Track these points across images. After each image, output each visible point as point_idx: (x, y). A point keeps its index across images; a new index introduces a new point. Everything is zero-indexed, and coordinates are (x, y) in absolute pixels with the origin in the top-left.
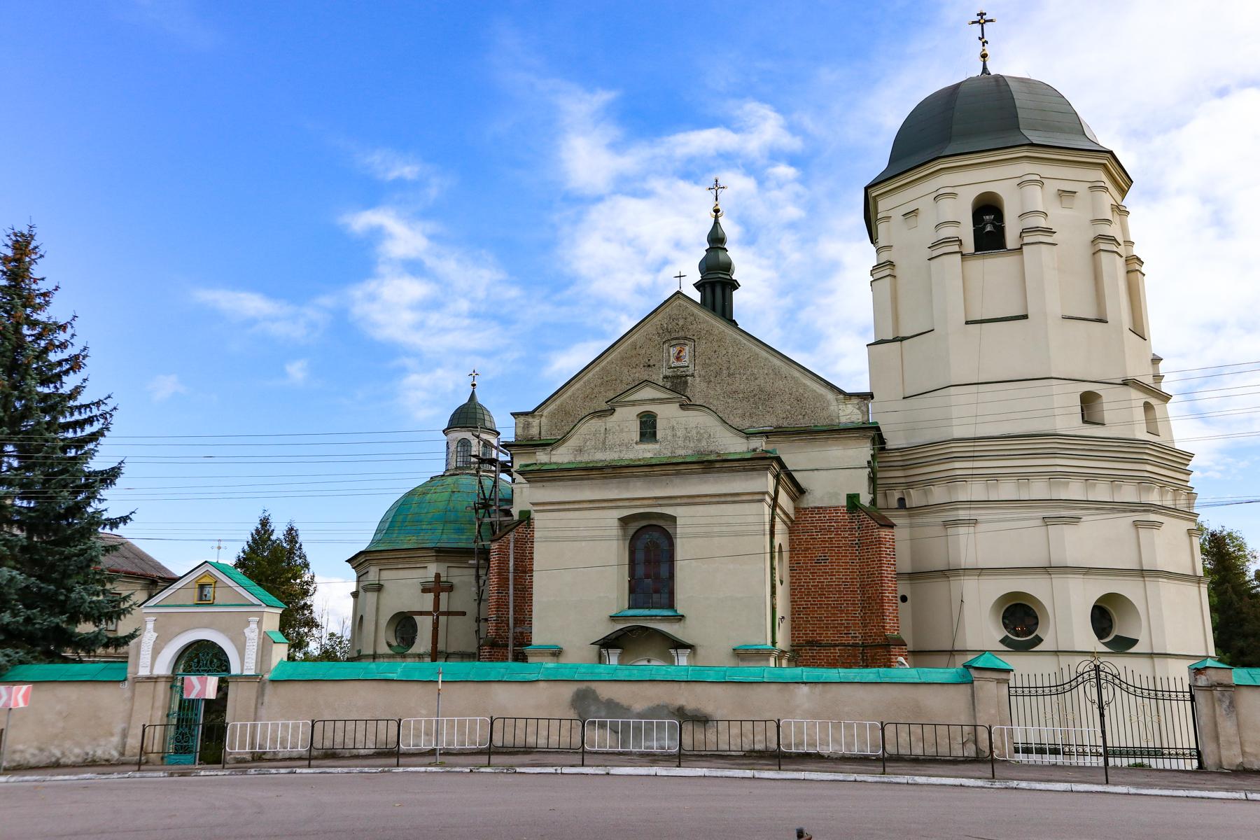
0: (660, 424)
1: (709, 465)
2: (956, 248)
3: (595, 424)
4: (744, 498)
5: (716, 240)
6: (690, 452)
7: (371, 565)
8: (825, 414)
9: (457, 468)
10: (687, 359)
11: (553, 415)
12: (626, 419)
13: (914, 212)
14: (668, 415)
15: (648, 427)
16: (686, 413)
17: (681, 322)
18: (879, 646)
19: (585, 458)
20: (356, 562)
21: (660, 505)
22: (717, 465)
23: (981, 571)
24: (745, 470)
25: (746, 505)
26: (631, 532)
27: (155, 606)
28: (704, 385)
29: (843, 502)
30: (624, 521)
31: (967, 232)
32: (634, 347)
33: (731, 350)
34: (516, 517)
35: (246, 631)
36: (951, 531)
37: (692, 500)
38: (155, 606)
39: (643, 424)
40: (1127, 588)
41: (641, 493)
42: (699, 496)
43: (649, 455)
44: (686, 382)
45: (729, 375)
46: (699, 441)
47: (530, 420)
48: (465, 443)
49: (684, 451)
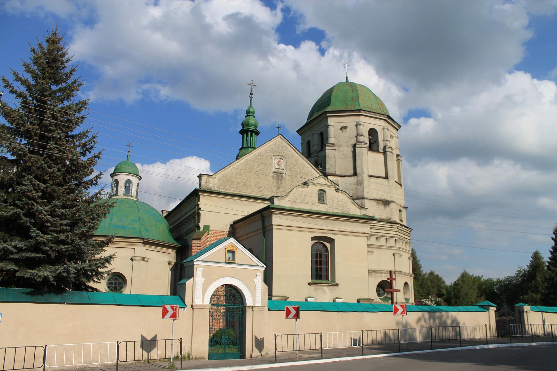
1: (351, 218)
6: (339, 212)
12: (313, 190)
13: (347, 127)
14: (330, 192)
15: (321, 197)
16: (337, 193)
17: (281, 149)
21: (329, 233)
28: (290, 179)
35: (255, 280)
37: (342, 232)
41: (323, 227)
43: (323, 210)
44: (282, 176)
47: (210, 179)
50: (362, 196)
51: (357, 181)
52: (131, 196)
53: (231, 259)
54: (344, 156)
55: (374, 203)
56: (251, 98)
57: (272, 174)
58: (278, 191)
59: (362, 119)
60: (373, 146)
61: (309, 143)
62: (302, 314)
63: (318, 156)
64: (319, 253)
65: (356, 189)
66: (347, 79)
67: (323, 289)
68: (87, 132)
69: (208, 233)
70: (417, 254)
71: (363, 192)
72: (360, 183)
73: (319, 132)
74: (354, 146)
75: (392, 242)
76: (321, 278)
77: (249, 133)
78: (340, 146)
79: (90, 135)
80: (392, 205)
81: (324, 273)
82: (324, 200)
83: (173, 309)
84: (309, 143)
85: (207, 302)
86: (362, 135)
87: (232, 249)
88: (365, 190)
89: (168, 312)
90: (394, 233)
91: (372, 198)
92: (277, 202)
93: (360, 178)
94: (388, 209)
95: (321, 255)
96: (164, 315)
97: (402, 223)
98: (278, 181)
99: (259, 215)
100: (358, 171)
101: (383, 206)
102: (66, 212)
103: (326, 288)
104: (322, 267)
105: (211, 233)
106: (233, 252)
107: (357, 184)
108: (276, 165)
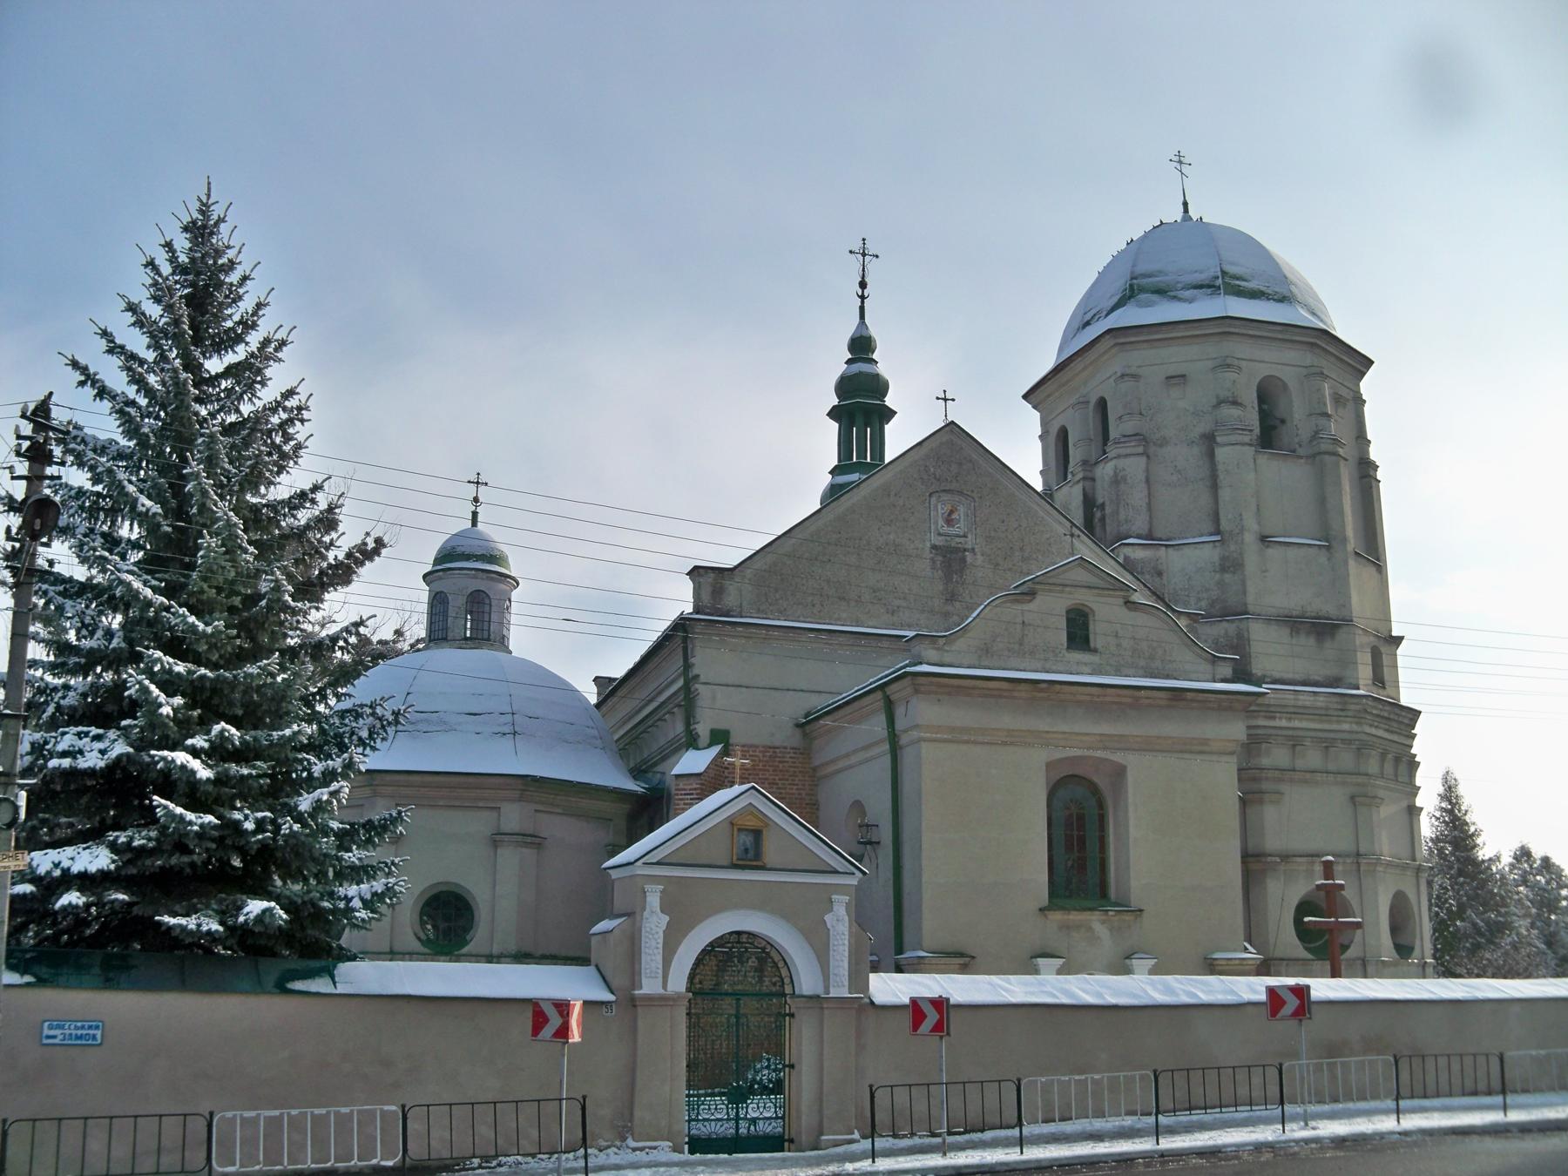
2: (1247, 439)
5: (861, 346)
14: (1107, 615)
15: (1079, 631)
16: (1133, 614)
23: (1286, 857)
27: (658, 863)
30: (1050, 766)
31: (1252, 418)
35: (826, 918)
37: (1148, 746)
38: (658, 863)
39: (1071, 622)
44: (964, 560)
51: (1223, 559)
53: (751, 854)
56: (863, 298)
57: (927, 554)
58: (950, 608)
59: (1240, 349)
60: (1269, 435)
61: (1063, 435)
62: (955, 1020)
63: (1093, 480)
66: (1186, 210)
67: (1090, 929)
68: (316, 488)
70: (1462, 790)
71: (1245, 593)
72: (1230, 565)
73: (1093, 400)
74: (1209, 440)
75: (1346, 760)
77: (860, 420)
78: (1164, 442)
79: (323, 501)
80: (1342, 635)
82: (1087, 640)
83: (561, 1015)
84: (1063, 435)
85: (678, 982)
86: (1235, 403)
87: (752, 823)
88: (1251, 589)
89: (546, 1020)
90: (1355, 727)
93: (1232, 548)
95: (1081, 818)
96: (536, 1030)
98: (948, 578)
99: (879, 695)
101: (1312, 641)
102: (255, 739)
106: (757, 834)
107: (1223, 569)
108: (941, 522)
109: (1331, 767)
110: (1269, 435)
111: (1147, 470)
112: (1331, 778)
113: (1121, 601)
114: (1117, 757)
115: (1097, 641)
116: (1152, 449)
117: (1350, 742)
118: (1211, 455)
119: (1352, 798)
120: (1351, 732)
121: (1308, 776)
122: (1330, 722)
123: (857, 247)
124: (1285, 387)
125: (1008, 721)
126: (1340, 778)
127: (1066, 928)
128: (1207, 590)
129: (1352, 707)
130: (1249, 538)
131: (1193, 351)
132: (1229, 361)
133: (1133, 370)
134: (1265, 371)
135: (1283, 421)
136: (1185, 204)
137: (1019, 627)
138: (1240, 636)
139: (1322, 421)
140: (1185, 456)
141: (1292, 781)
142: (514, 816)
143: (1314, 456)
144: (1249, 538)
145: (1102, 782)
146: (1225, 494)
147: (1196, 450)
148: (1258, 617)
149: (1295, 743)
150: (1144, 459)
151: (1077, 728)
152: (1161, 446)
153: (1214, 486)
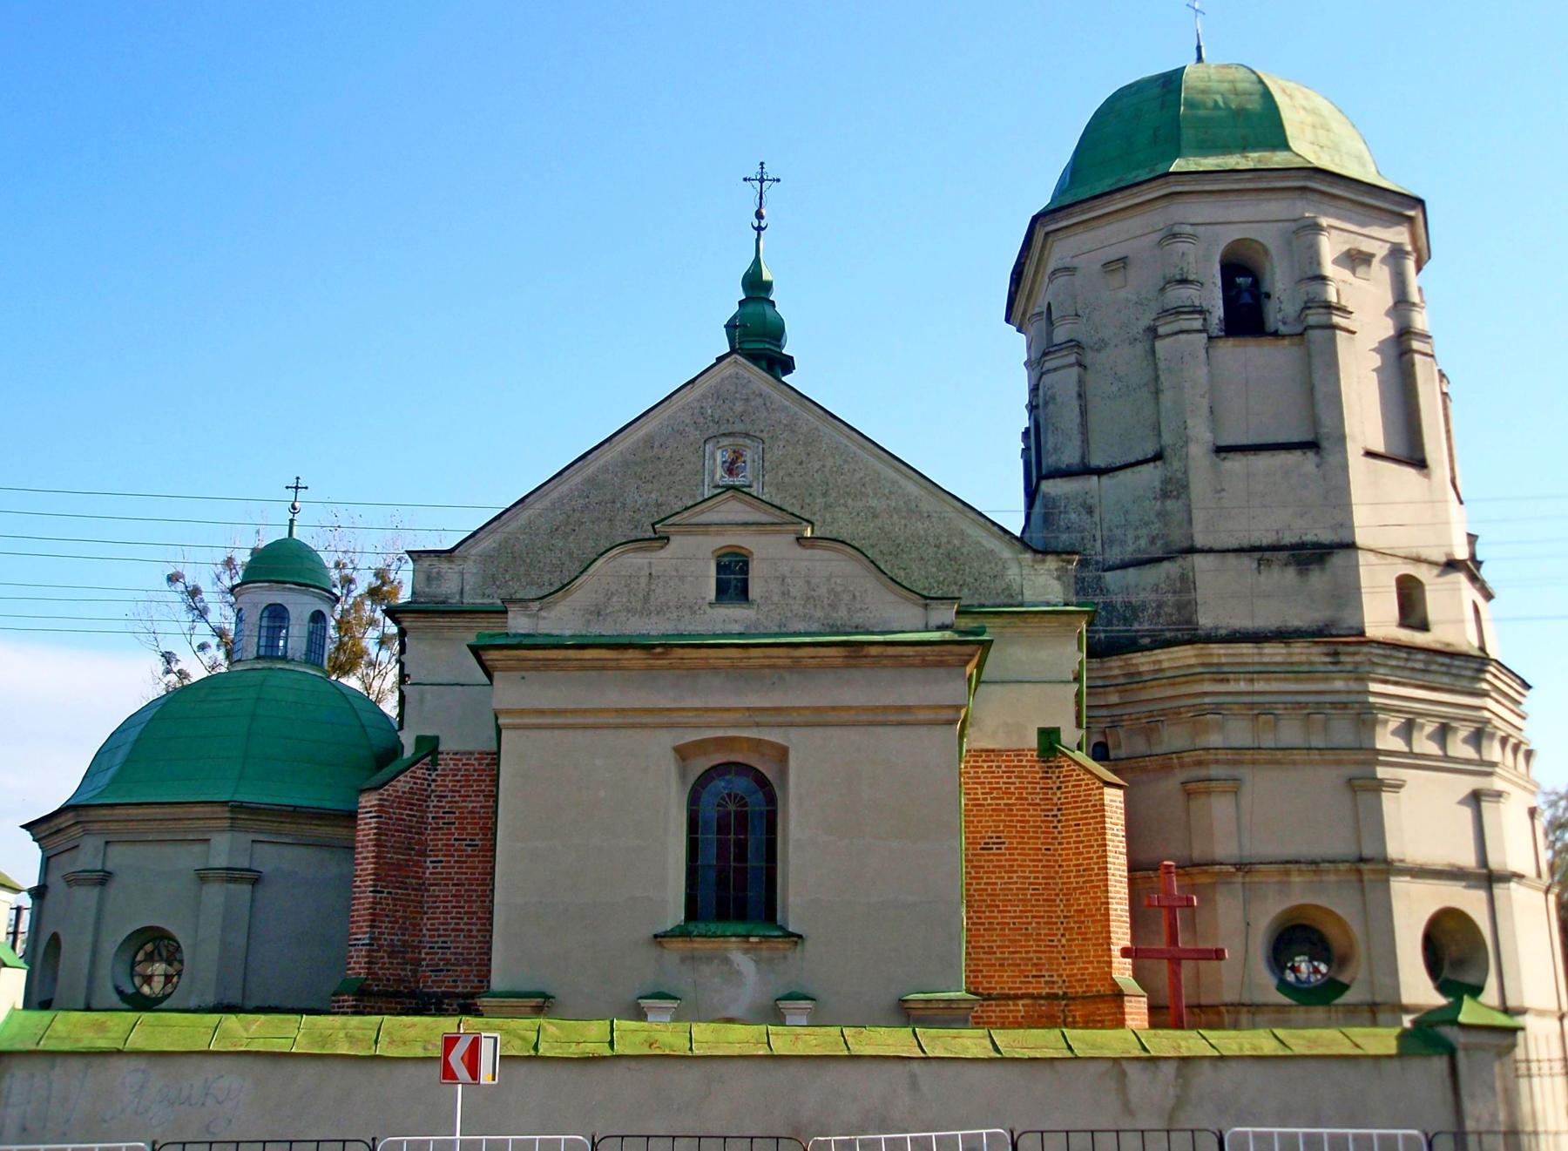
0: (755, 570)
2: (1198, 324)
3: (637, 561)
4: (922, 716)
5: (756, 287)
7: (87, 832)
8: (999, 585)
9: (258, 657)
10: (748, 473)
11: (487, 558)
12: (691, 561)
13: (1123, 261)
14: (770, 555)
15: (733, 579)
17: (739, 407)
18: (1100, 997)
19: (607, 628)
20: (44, 830)
21: (758, 725)
22: (874, 651)
24: (925, 664)
25: (923, 731)
26: (692, 779)
29: (1033, 742)
30: (683, 753)
32: (649, 441)
33: (830, 462)
34: (409, 751)
36: (1194, 805)
37: (820, 718)
40: (1471, 902)
42: (834, 709)
45: (828, 506)
46: (833, 607)
47: (444, 566)
48: (277, 615)
49: (802, 627)
50: (1185, 544)
51: (1166, 481)
52: (284, 658)
54: (1114, 388)
55: (1248, 562)
56: (759, 229)
64: (732, 808)
65: (1162, 515)
69: (434, 765)
71: (1190, 521)
72: (1175, 489)
75: (1342, 732)
76: (742, 916)
78: (1102, 345)
80: (1338, 559)
81: (754, 893)
86: (1184, 281)
88: (1199, 517)
90: (1354, 686)
91: (1234, 544)
92: (518, 623)
93: (1176, 464)
94: (1318, 579)
95: (742, 818)
97: (1419, 638)
100: (1167, 438)
103: (742, 961)
104: (734, 871)
105: (446, 763)
107: (1165, 495)
108: (719, 472)
109: (1317, 742)
110: (1246, 313)
111: (1081, 382)
112: (1315, 756)
113: (793, 536)
114: (774, 736)
115: (755, 591)
116: (1089, 358)
117: (1345, 705)
118: (1153, 351)
119: (1350, 782)
120: (1349, 692)
121: (1279, 755)
122: (1313, 680)
123: (753, 172)
124: (1266, 251)
125: (614, 695)
126: (1329, 756)
127: (690, 959)
128: (1147, 524)
129: (1348, 659)
130: (1198, 452)
131: (1135, 224)
132: (1177, 229)
133: (1067, 262)
134: (1235, 233)
135: (1268, 296)
136: (1199, 48)
137: (643, 581)
138: (1183, 578)
139: (1314, 287)
140: (1122, 359)
141: (1254, 762)
142: (224, 849)
143: (1301, 334)
144: (1198, 452)
145: (700, 765)
146: (1167, 398)
147: (1140, 348)
148: (1211, 551)
149: (1259, 711)
150: (1076, 369)
151: (712, 703)
152: (1098, 351)
153: (1157, 393)
